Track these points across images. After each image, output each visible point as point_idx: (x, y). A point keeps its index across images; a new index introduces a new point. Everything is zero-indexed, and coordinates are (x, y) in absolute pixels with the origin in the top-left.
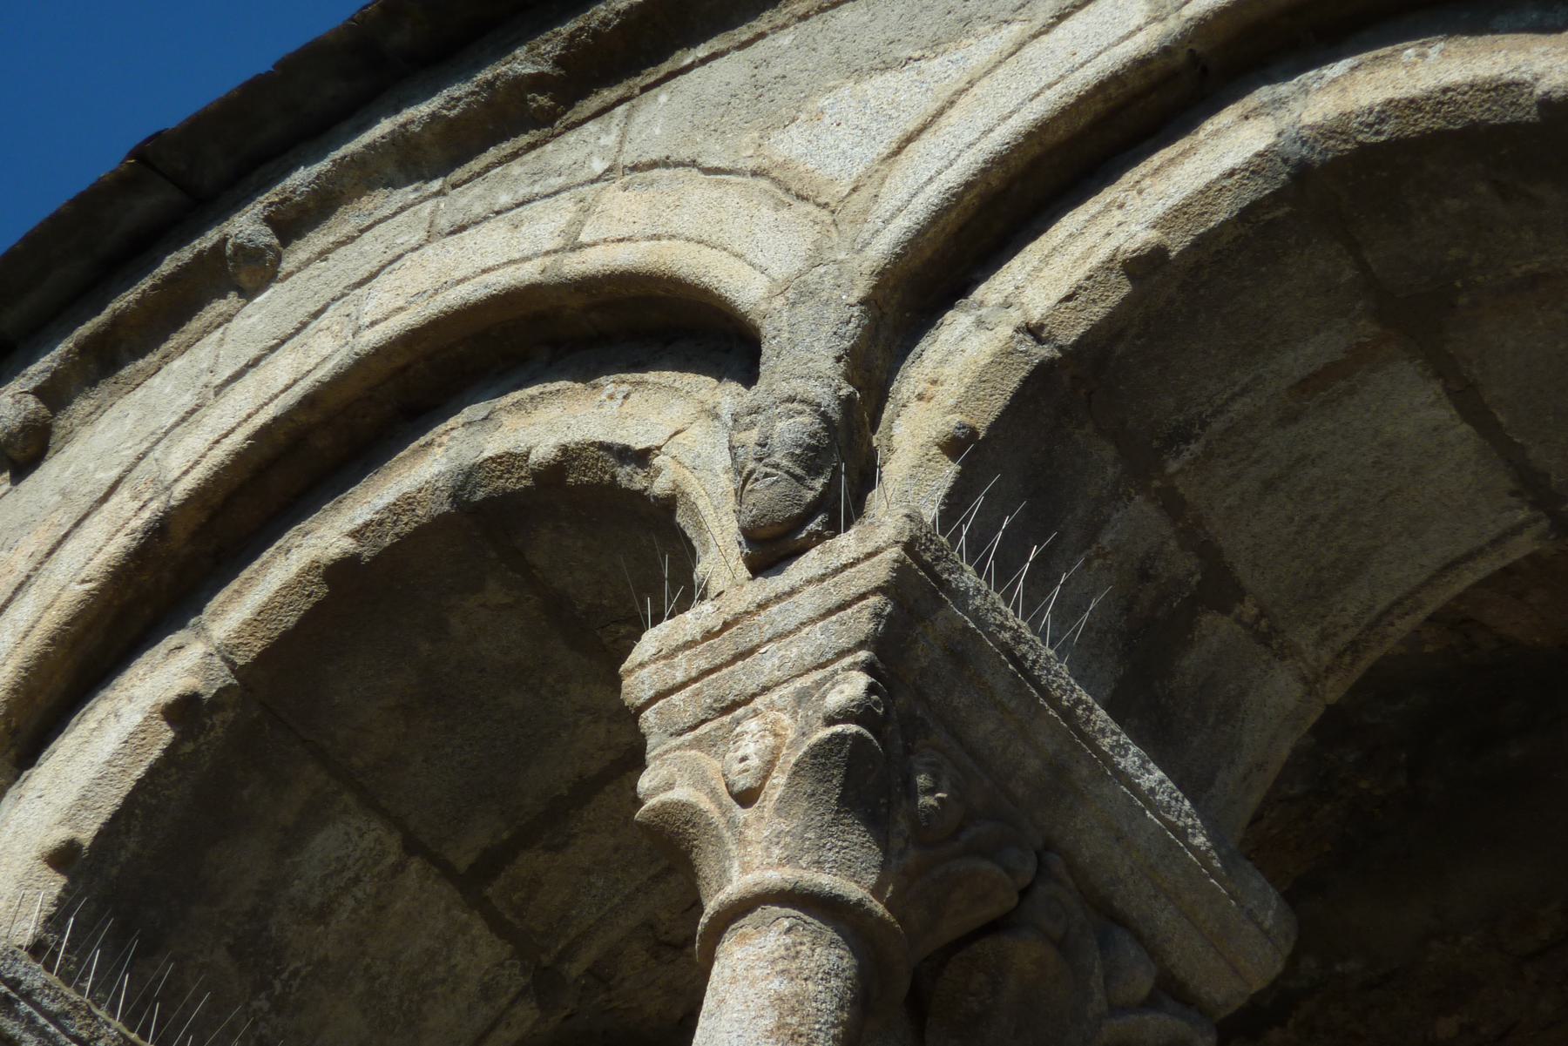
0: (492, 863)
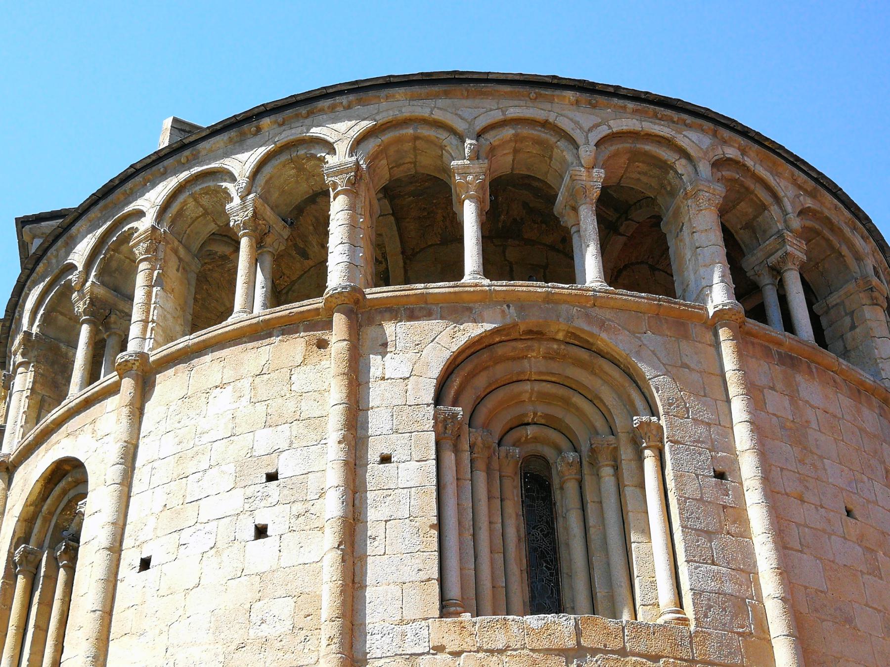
0: (392, 168)
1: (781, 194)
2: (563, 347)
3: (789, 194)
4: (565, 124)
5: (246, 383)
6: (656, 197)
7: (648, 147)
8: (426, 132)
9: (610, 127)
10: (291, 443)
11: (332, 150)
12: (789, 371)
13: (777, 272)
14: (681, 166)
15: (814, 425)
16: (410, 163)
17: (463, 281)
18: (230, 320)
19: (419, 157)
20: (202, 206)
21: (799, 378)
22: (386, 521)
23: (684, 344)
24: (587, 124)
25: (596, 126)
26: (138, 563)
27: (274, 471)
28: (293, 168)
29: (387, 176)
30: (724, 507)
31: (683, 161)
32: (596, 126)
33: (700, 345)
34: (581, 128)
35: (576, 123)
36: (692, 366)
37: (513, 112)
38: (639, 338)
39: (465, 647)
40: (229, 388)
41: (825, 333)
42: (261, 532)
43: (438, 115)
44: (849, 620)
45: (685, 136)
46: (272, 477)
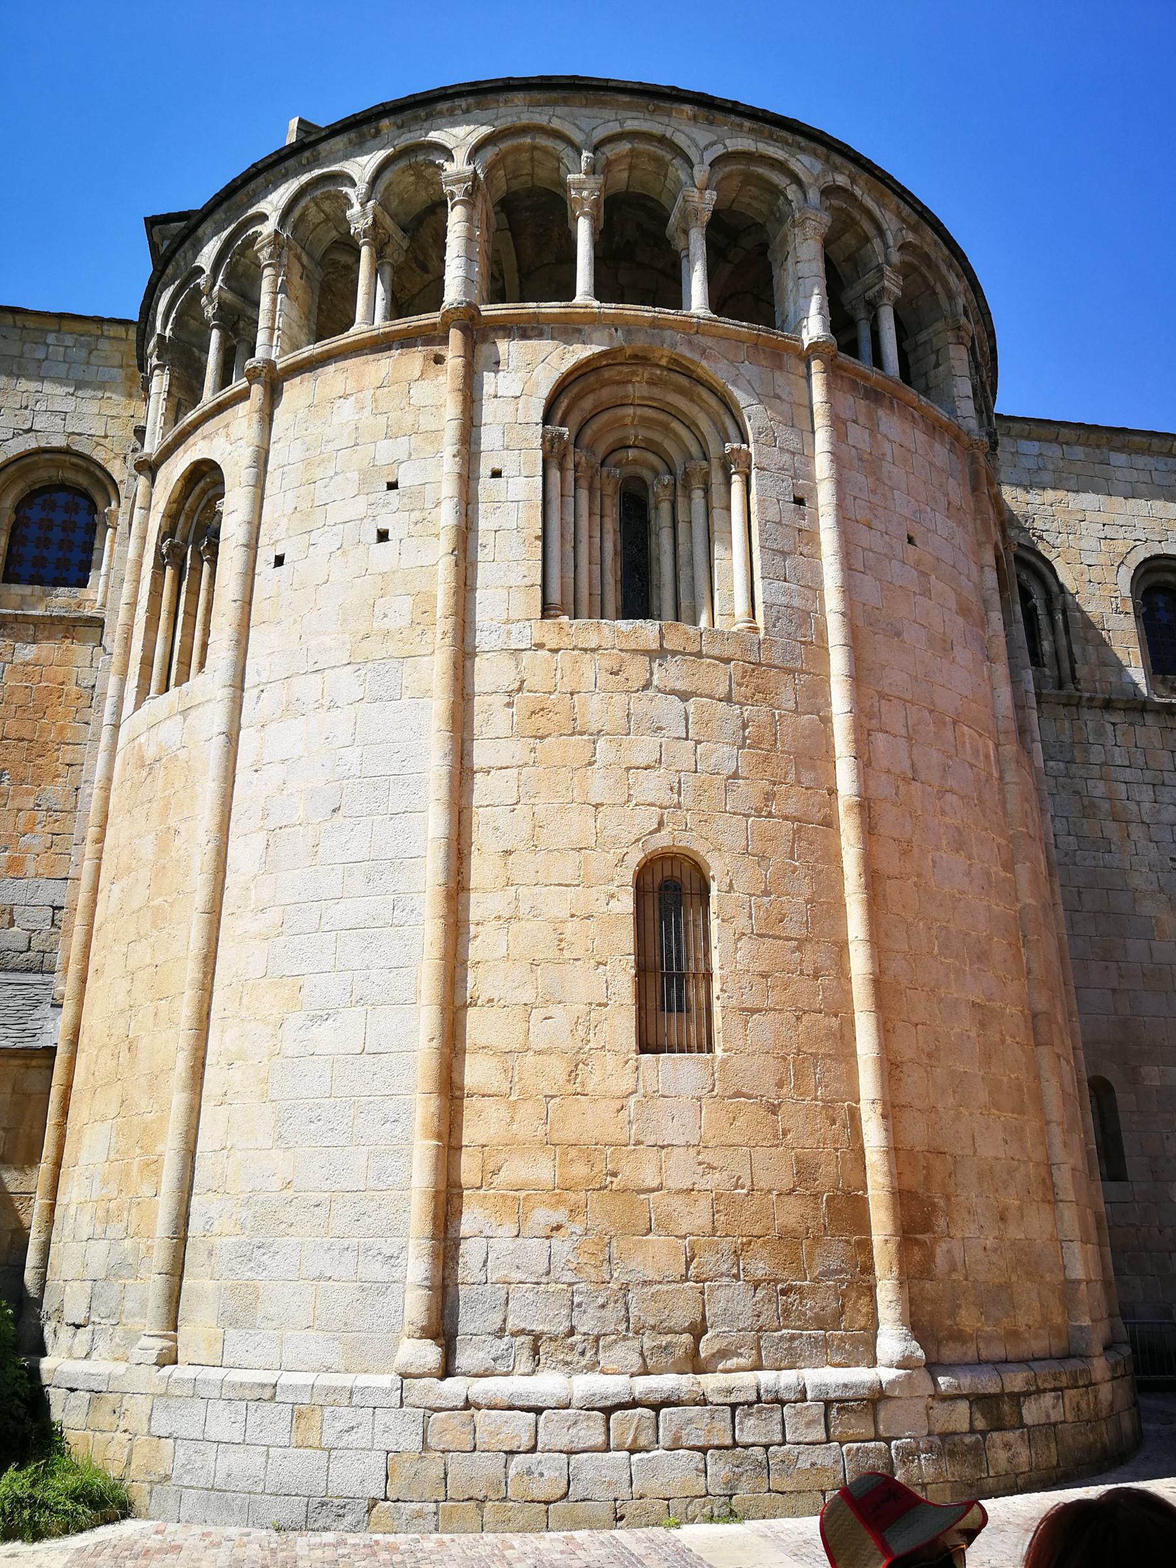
1: (885, 227)
2: (665, 373)
3: (892, 228)
4: (681, 140)
5: (368, 394)
6: (765, 223)
7: (762, 170)
8: (543, 141)
9: (725, 147)
10: (410, 454)
11: (450, 157)
12: (873, 406)
13: (873, 307)
14: (792, 192)
15: (889, 458)
16: (527, 174)
17: (574, 301)
18: (352, 331)
19: (536, 169)
20: (323, 211)
21: (881, 412)
22: (496, 531)
23: (778, 374)
24: (702, 145)
25: (713, 144)
26: (273, 560)
27: (394, 480)
28: (412, 175)
29: (505, 188)
30: (800, 530)
31: (794, 187)
32: (713, 144)
33: (793, 377)
34: (697, 146)
35: (693, 140)
36: (784, 397)
37: (631, 125)
38: (737, 368)
39: (562, 645)
40: (352, 399)
41: (911, 369)
42: (383, 536)
43: (556, 124)
44: (898, 634)
45: (798, 159)
46: (392, 486)
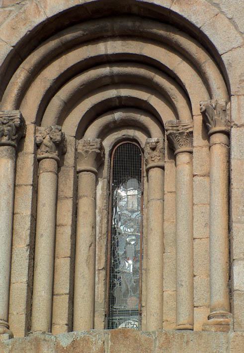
2: (137, 24)
